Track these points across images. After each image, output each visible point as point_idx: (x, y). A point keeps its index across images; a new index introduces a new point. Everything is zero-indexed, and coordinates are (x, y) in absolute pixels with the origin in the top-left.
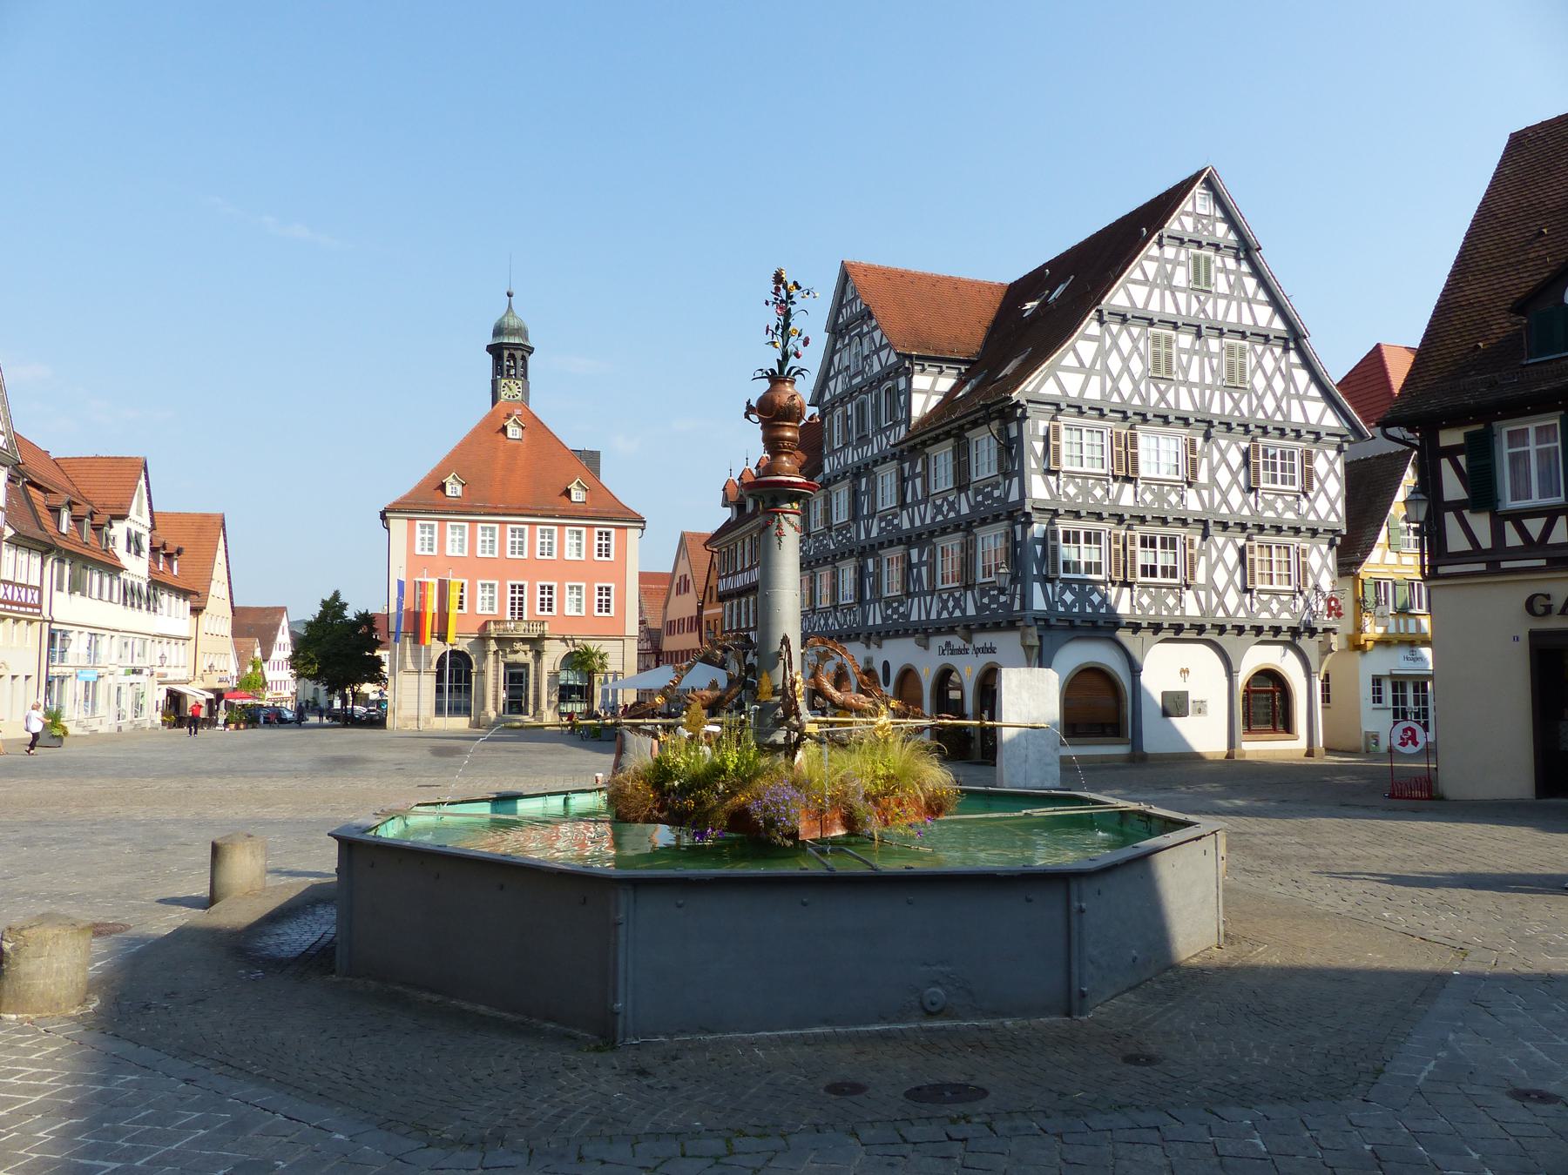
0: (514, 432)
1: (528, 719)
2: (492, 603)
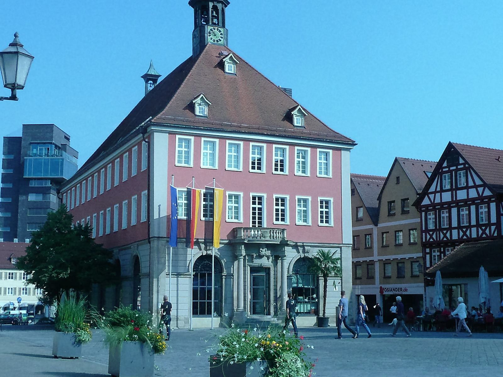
0: (230, 68)
2: (237, 213)
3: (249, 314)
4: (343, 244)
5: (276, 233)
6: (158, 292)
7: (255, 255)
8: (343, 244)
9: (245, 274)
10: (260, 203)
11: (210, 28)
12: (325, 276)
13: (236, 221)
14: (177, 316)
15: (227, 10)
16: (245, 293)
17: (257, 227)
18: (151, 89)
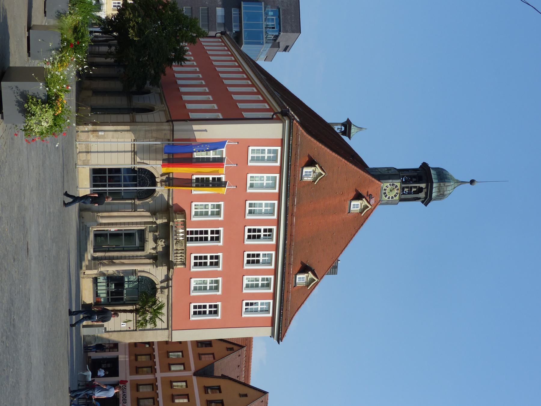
0: (356, 206)
1: (90, 253)
2: (201, 214)
3: (93, 229)
4: (172, 330)
5: (181, 256)
6: (116, 131)
7: (157, 234)
8: (172, 330)
9: (137, 223)
10: (212, 239)
11: (398, 185)
12: (136, 311)
13: (193, 213)
14: (91, 152)
15: (419, 203)
16: (116, 224)
17: (187, 236)
18: (336, 129)
